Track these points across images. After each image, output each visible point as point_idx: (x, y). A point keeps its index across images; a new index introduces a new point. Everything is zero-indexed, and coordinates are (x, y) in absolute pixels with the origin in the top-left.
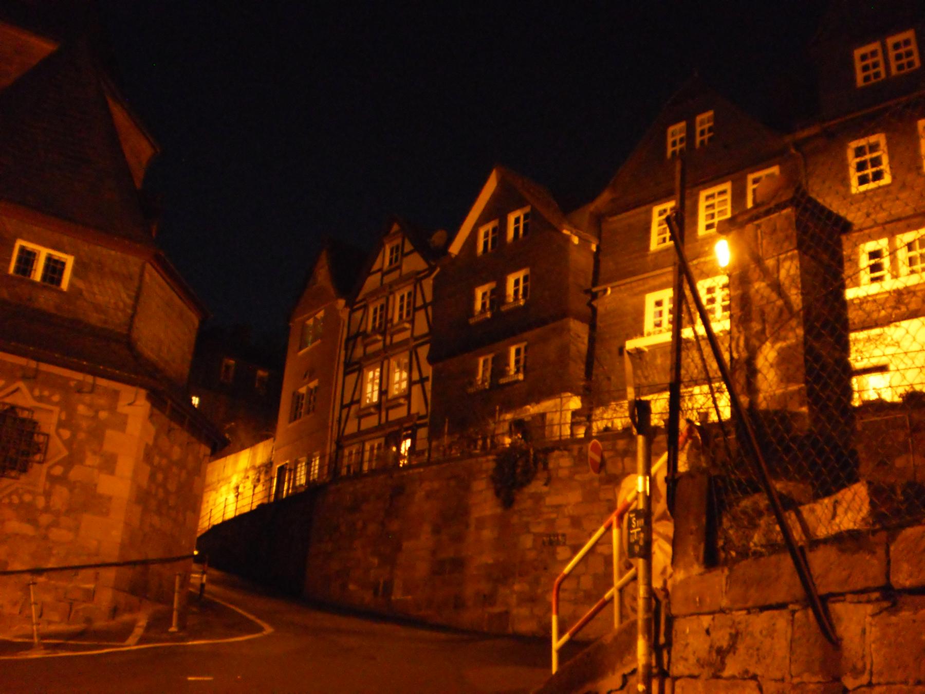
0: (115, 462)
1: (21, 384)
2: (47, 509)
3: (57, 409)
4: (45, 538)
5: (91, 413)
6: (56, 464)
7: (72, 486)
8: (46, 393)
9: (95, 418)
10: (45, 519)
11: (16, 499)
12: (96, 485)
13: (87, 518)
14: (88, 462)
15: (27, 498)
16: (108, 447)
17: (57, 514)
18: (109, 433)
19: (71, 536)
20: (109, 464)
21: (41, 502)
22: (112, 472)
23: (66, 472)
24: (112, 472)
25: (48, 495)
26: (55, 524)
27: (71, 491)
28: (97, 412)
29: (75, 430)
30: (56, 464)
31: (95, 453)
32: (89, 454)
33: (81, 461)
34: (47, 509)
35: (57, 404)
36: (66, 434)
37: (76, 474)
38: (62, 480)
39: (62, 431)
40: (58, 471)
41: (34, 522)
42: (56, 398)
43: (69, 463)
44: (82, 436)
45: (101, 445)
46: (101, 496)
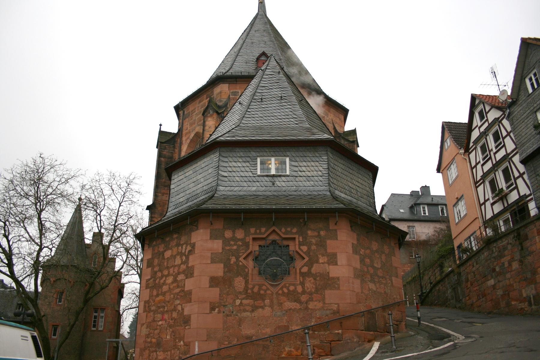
0: (336, 258)
1: (274, 228)
2: (304, 292)
3: (297, 236)
4: (307, 308)
5: (316, 234)
6: (303, 266)
7: (315, 276)
8: (289, 229)
9: (319, 236)
10: (304, 298)
11: (285, 290)
12: (328, 273)
13: (328, 292)
14: (321, 261)
15: (292, 288)
16: (329, 251)
17: (311, 294)
18: (328, 242)
19: (321, 304)
20: (333, 260)
21: (300, 289)
22: (336, 264)
23: (310, 270)
24: (336, 264)
25: (302, 284)
26: (311, 300)
27: (315, 279)
28: (319, 233)
29: (309, 245)
30: (303, 266)
31: (323, 255)
32: (320, 256)
33: (317, 262)
34: (304, 292)
35: (296, 233)
36: (305, 248)
37: (315, 269)
38: (309, 274)
39: (302, 247)
40: (305, 269)
41: (298, 301)
42: (295, 230)
43: (310, 264)
44: (313, 247)
45: (326, 250)
46: (333, 278)
